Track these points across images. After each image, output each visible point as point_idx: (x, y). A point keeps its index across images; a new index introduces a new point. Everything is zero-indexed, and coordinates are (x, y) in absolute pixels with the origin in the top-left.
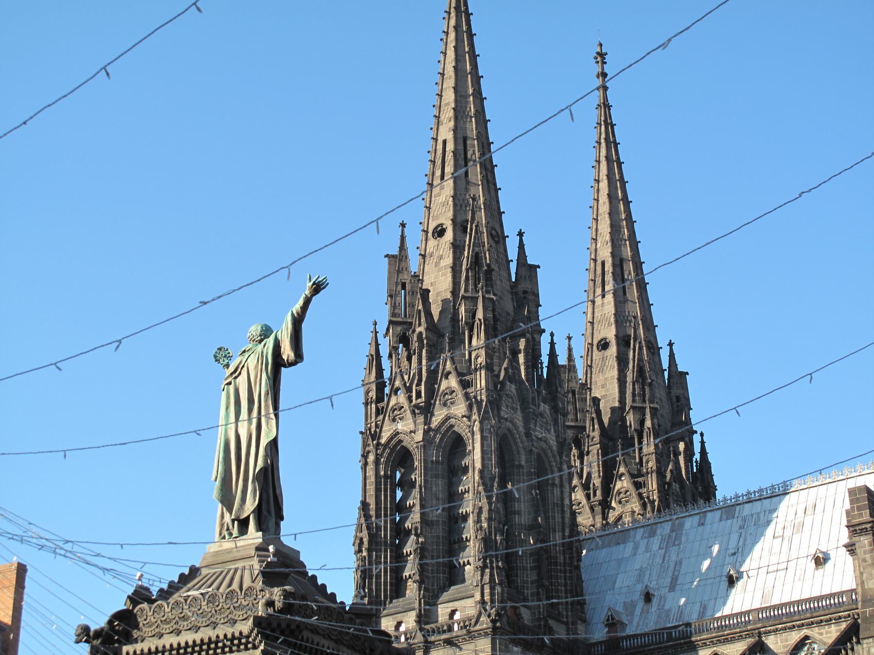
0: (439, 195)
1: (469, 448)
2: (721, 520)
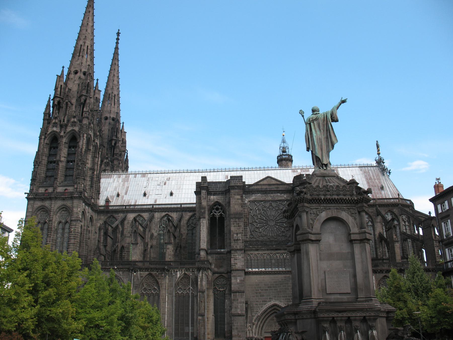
0: (77, 61)
1: (78, 141)
2: (141, 177)
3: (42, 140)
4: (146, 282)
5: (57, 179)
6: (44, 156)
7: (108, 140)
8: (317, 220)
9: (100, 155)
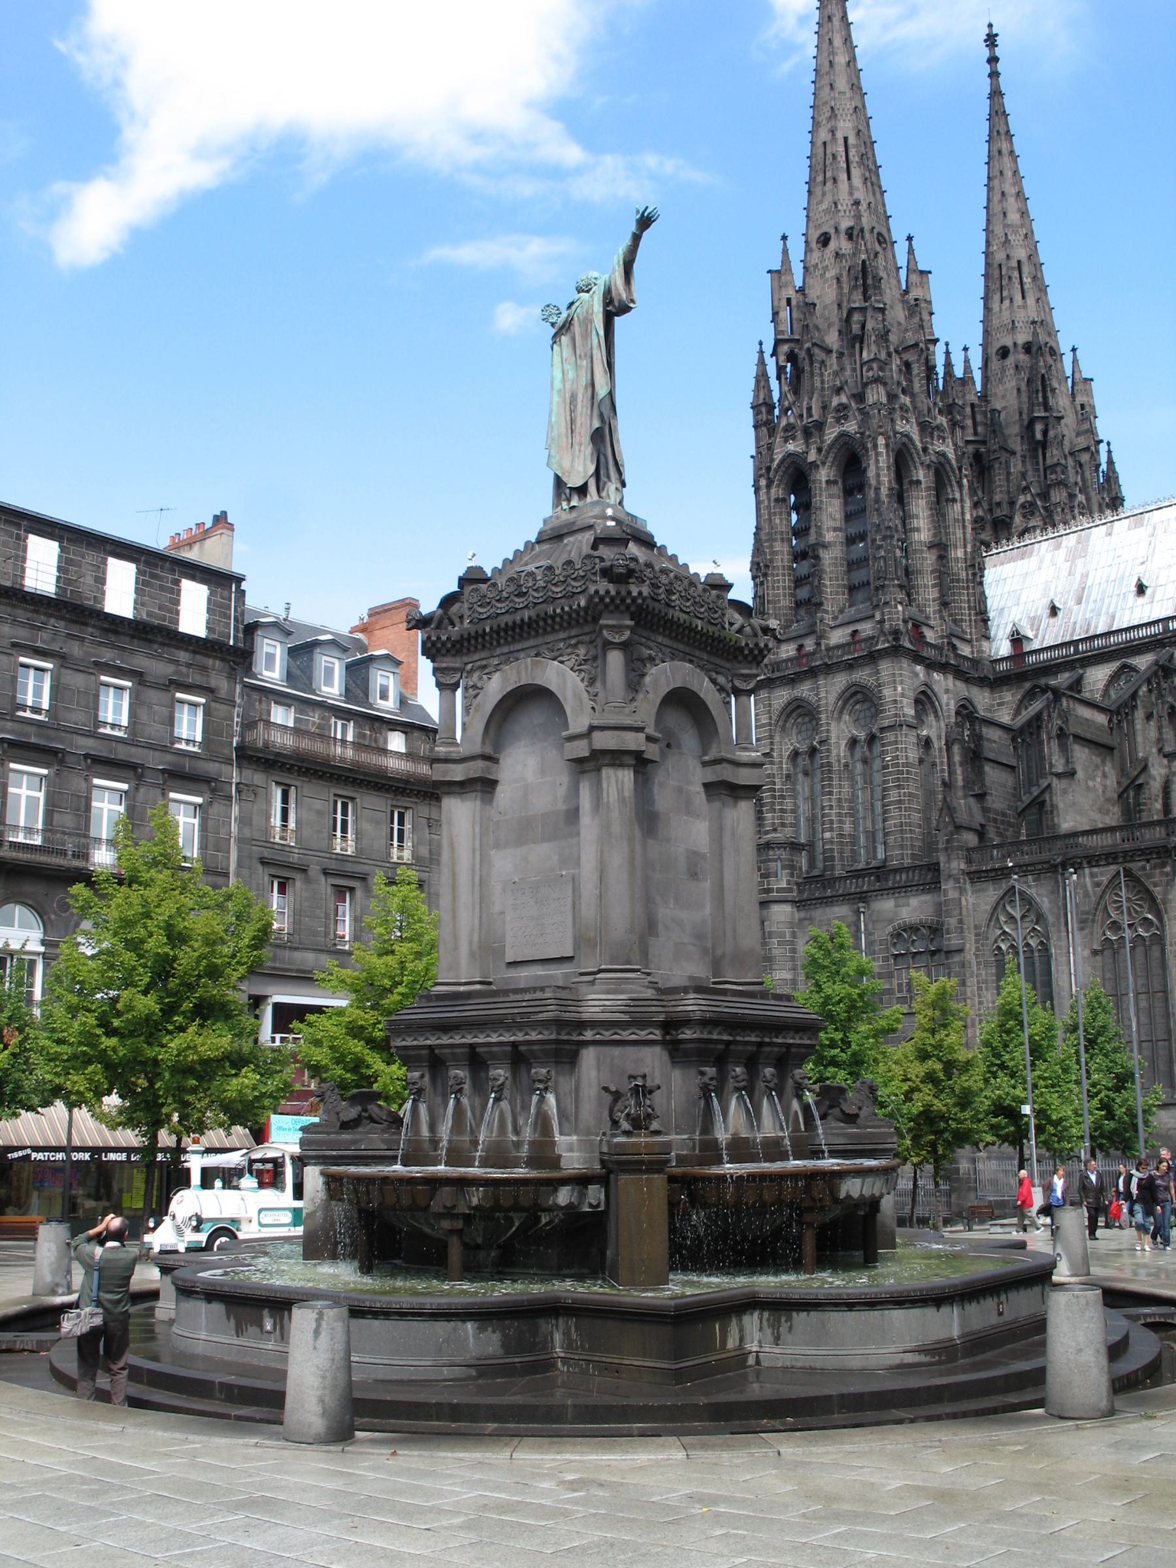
0: (821, 202)
3: (763, 491)
4: (1116, 902)
5: (821, 604)
6: (776, 540)
7: (1021, 426)
8: (476, 710)
9: (966, 490)
